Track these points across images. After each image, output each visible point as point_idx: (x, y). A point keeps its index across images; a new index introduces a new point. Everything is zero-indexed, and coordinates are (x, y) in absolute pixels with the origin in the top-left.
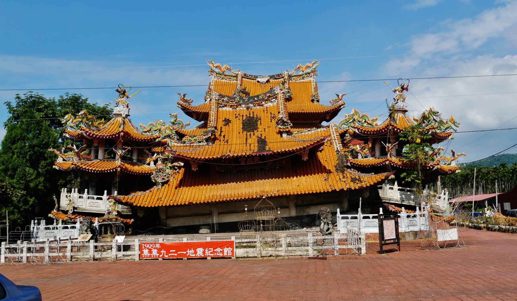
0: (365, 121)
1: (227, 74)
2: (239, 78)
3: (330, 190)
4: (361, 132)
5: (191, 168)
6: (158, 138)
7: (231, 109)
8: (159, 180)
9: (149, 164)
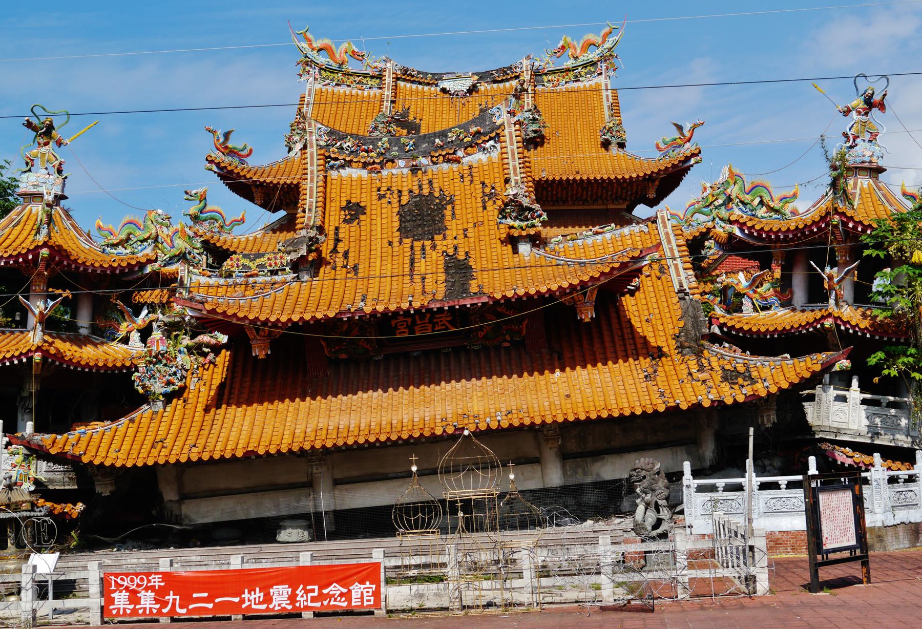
0: (762, 203)
1: (350, 70)
2: (388, 80)
3: (661, 408)
4: (750, 235)
5: (249, 349)
6: (149, 261)
7: (364, 173)
8: (158, 387)
9: (126, 340)
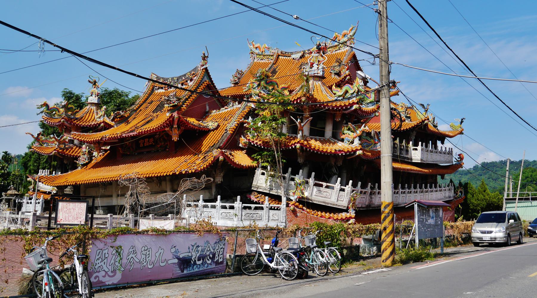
1: (266, 54)
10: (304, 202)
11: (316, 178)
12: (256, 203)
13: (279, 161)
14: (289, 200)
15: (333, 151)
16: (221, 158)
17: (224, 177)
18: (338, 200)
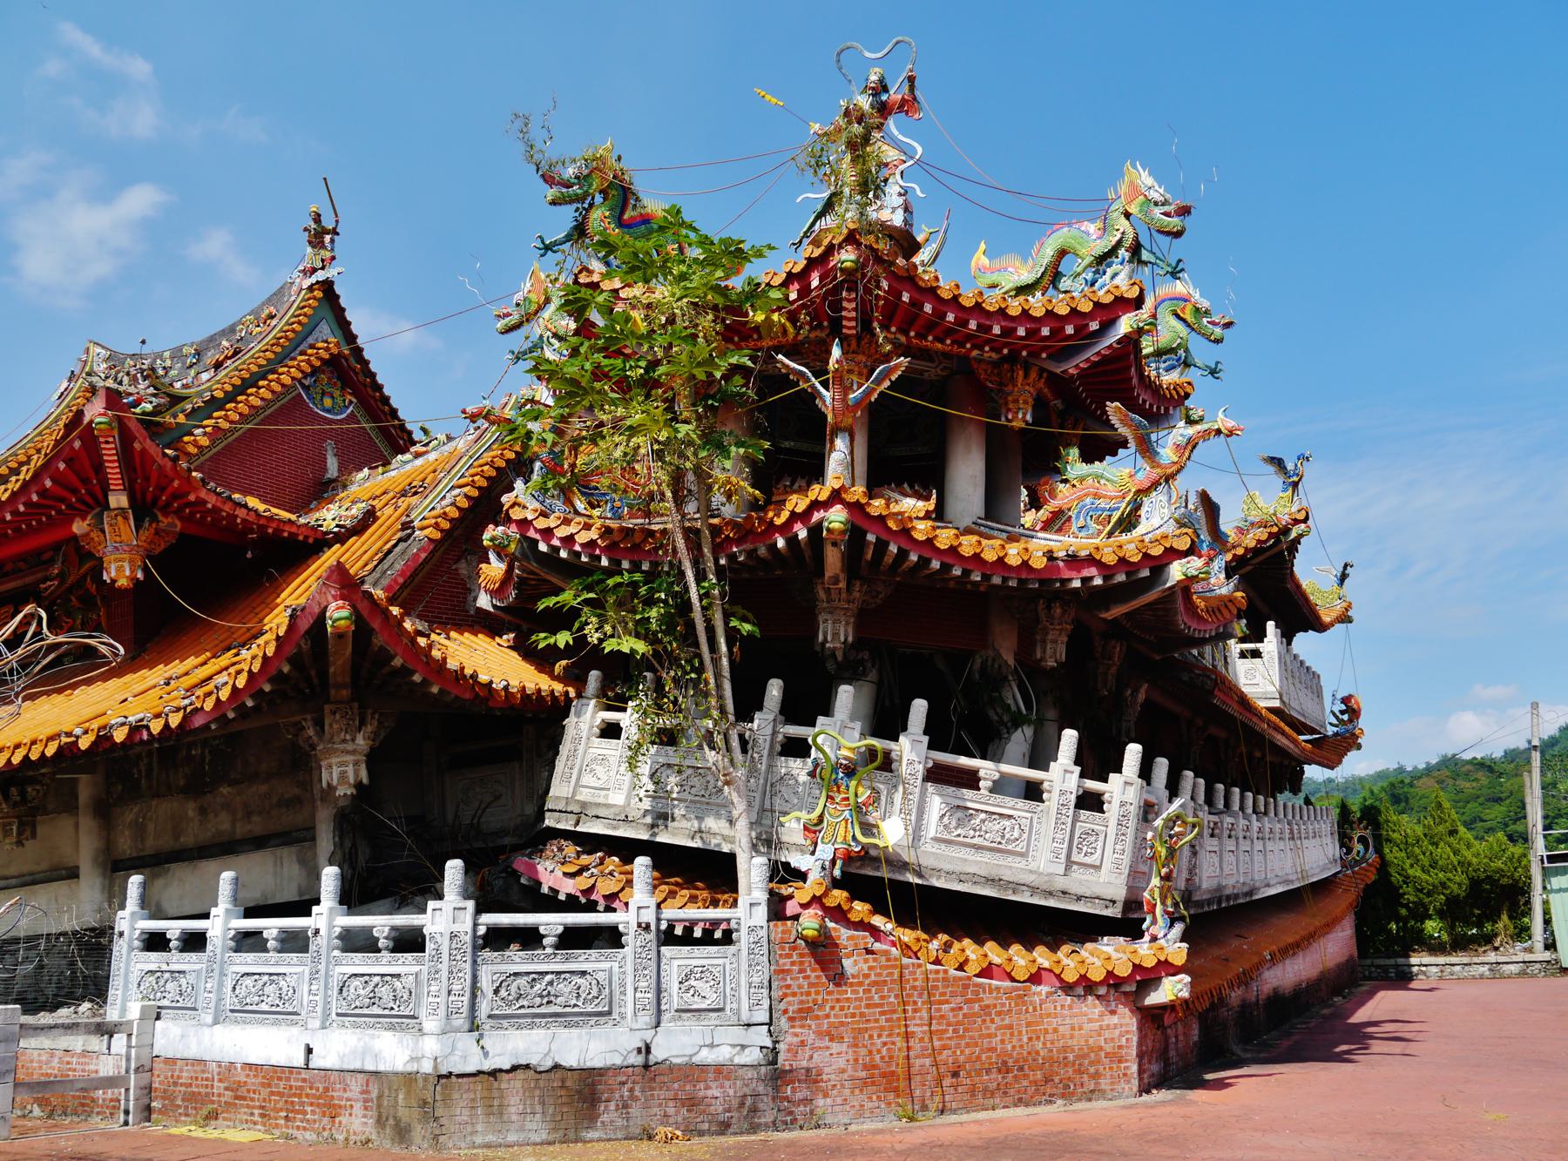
10: (872, 883)
11: (938, 736)
12: (572, 904)
13: (710, 630)
14: (783, 874)
15: (1039, 562)
16: (338, 613)
17: (373, 759)
18: (1069, 863)
